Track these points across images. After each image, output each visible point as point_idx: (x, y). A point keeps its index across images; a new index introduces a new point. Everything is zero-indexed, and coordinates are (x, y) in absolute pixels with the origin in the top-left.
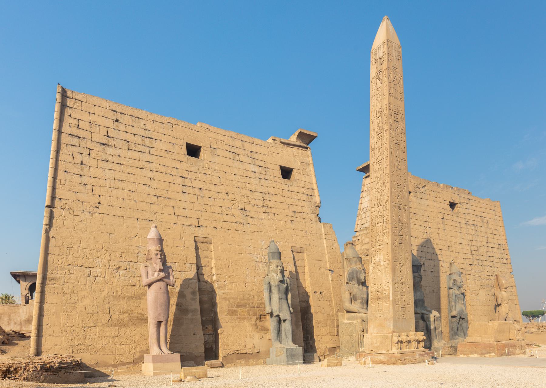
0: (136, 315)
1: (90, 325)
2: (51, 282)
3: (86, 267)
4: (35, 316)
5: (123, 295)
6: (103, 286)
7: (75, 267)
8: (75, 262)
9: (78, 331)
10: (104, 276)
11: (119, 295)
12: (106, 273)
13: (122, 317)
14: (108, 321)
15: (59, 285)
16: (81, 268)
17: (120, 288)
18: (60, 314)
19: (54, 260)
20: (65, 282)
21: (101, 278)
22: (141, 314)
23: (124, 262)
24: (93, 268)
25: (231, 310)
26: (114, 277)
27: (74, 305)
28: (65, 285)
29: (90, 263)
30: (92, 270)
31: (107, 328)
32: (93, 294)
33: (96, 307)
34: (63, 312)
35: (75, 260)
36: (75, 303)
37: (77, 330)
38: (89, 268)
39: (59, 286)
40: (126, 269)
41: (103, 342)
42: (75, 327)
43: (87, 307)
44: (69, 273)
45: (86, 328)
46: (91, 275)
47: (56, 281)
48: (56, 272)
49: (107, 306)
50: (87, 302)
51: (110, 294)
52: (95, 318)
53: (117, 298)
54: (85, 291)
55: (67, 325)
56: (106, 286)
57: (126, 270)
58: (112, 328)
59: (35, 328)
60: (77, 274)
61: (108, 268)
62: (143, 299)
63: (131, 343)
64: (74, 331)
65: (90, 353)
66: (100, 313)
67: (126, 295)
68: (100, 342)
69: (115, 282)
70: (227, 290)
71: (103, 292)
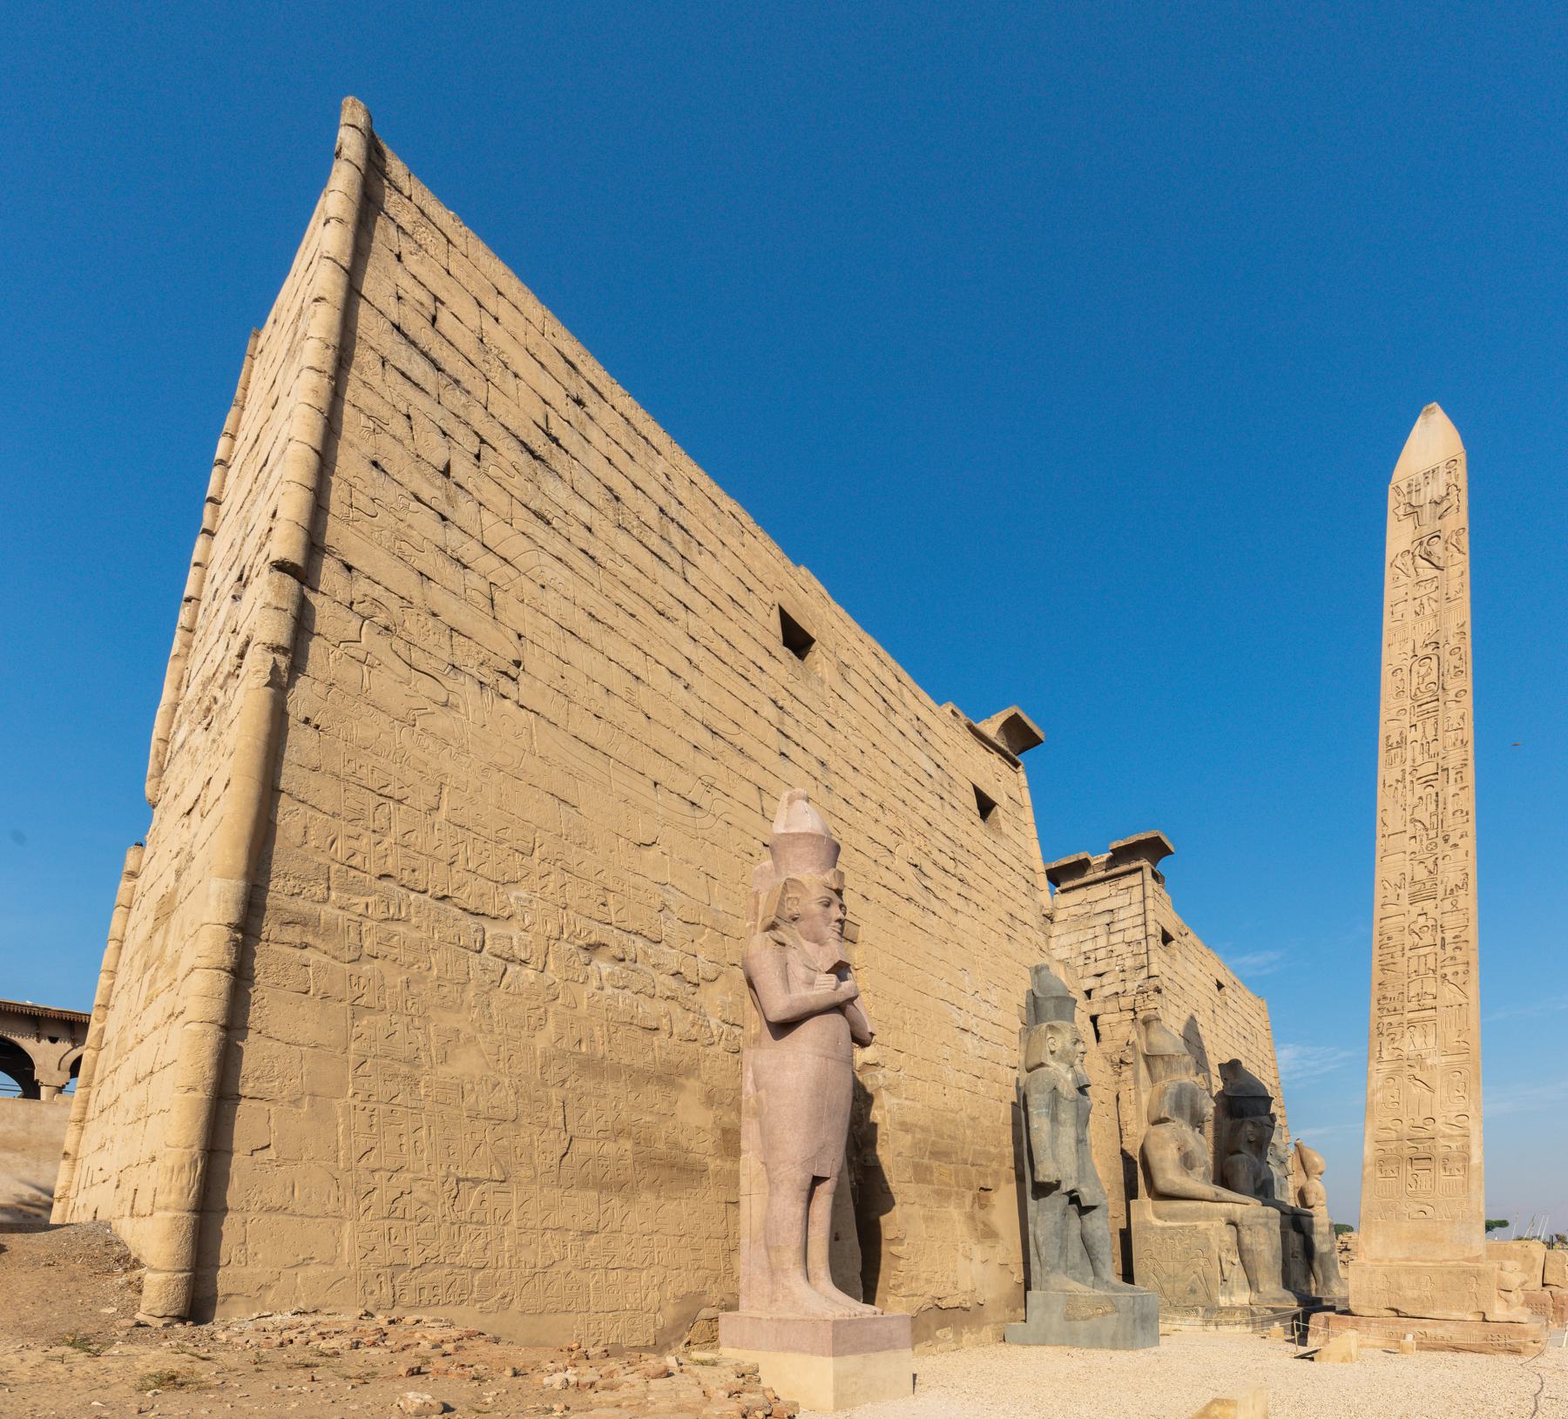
0: (661, 1147)
1: (484, 1174)
2: (292, 934)
3: (465, 910)
4: (192, 1094)
5: (616, 1060)
6: (538, 1008)
7: (413, 896)
8: (414, 871)
9: (425, 1197)
10: (540, 967)
11: (600, 1055)
12: (551, 956)
13: (609, 1148)
14: (556, 1161)
15: (335, 958)
16: (440, 904)
17: (605, 1029)
18: (335, 1102)
19: (312, 832)
20: (366, 951)
21: (529, 973)
22: (676, 1145)
23: (615, 931)
24: (494, 918)
25: (918, 1163)
26: (581, 980)
27: (404, 1069)
28: (366, 967)
29: (482, 895)
30: (492, 930)
31: (555, 1191)
32: (497, 1030)
33: (511, 1092)
34: (350, 1092)
35: (414, 864)
36: (413, 1061)
37: (420, 1192)
38: (478, 914)
39: (333, 962)
40: (623, 960)
41: (537, 1254)
42: (412, 1176)
43: (468, 1087)
44: (386, 915)
45: (461, 1184)
46: (487, 947)
47: (316, 935)
48: (319, 891)
49: (555, 1094)
50: (466, 1064)
51: (564, 1044)
52: (505, 1142)
53: (592, 1067)
54: (458, 1012)
55: (372, 1161)
56: (551, 1010)
57: (622, 964)
58: (573, 1192)
59: (187, 1160)
60: (424, 925)
61: (555, 934)
62: (682, 1087)
63: (646, 1264)
64: (406, 1197)
65: (478, 1306)
66: (525, 1121)
67: (626, 1061)
68: (526, 1255)
69: (586, 1000)
70: (906, 1099)
71: (538, 1034)
